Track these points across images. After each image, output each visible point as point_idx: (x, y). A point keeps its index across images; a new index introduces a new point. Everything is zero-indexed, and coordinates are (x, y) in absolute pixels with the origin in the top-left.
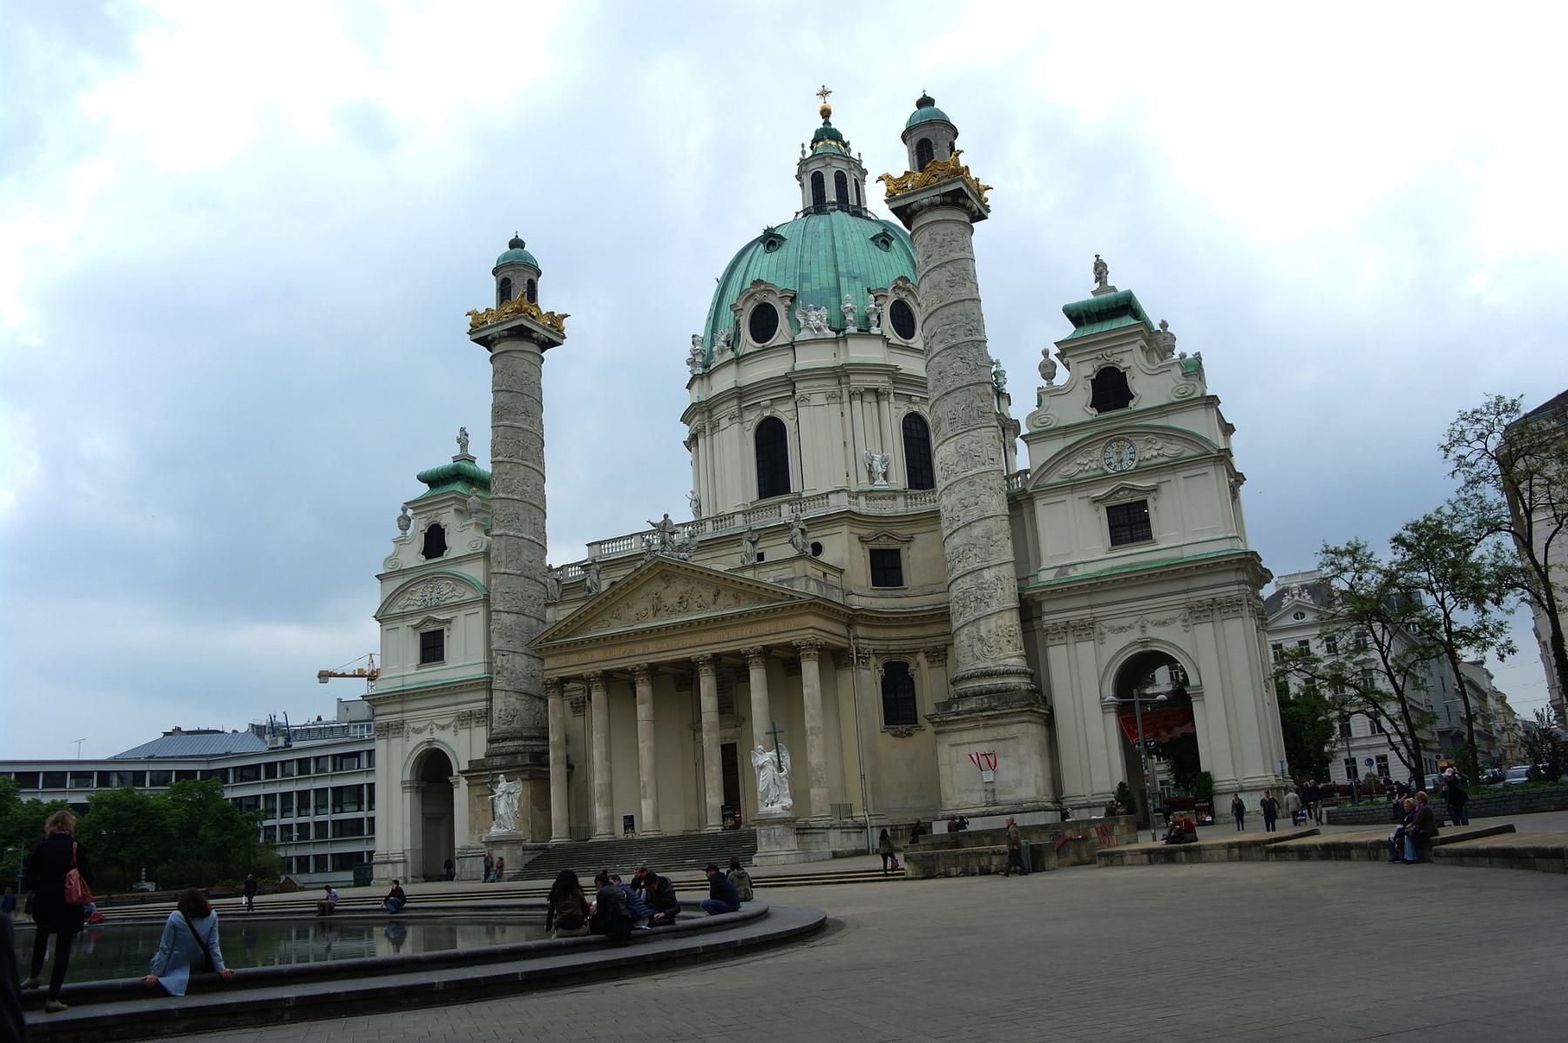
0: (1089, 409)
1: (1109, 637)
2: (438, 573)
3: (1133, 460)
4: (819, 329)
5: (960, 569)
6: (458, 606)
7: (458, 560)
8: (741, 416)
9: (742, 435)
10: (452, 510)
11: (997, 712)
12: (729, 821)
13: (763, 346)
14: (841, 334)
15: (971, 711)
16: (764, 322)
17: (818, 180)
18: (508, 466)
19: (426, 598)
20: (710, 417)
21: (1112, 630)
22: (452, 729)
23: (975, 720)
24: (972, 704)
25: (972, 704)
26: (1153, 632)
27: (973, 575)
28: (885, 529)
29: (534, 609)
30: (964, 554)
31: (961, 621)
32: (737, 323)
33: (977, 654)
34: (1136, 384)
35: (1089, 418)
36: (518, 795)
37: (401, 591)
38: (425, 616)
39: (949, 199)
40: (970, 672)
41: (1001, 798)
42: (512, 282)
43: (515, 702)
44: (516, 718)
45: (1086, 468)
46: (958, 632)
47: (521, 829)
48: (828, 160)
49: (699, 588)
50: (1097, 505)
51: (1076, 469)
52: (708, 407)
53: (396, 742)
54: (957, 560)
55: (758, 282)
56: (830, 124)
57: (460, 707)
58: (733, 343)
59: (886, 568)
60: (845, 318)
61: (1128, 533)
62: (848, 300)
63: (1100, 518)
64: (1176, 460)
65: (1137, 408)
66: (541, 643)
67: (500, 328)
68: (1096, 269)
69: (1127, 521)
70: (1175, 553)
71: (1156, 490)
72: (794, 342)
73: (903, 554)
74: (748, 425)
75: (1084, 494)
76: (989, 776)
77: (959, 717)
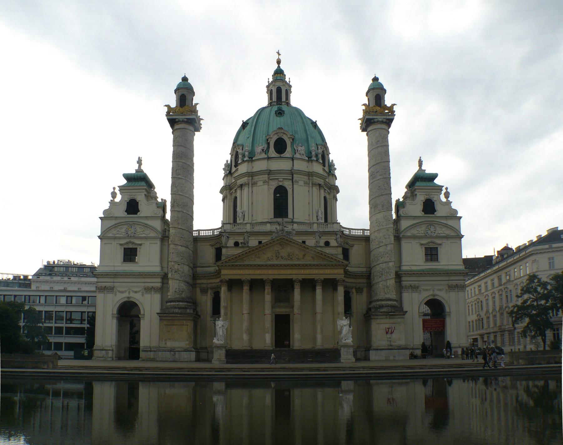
0: (421, 212)
2: (136, 222)
3: (435, 233)
4: (303, 155)
5: (381, 260)
6: (146, 238)
7: (146, 218)
8: (268, 182)
9: (269, 189)
11: (395, 313)
13: (280, 156)
14: (310, 159)
15: (384, 312)
16: (280, 146)
19: (128, 232)
20: (252, 179)
23: (386, 315)
24: (385, 310)
27: (386, 264)
28: (347, 240)
29: (191, 246)
30: (384, 256)
31: (380, 279)
33: (386, 292)
35: (422, 215)
37: (115, 226)
38: (129, 240)
40: (384, 298)
43: (183, 286)
44: (183, 294)
45: (420, 233)
46: (378, 283)
48: (284, 83)
50: (422, 246)
51: (416, 232)
52: (252, 175)
56: (280, 67)
58: (265, 151)
60: (311, 153)
61: (430, 257)
62: (312, 147)
63: (423, 251)
64: (448, 236)
65: (437, 215)
69: (430, 254)
70: (446, 268)
71: (441, 245)
72: (294, 157)
75: (417, 241)
77: (381, 314)
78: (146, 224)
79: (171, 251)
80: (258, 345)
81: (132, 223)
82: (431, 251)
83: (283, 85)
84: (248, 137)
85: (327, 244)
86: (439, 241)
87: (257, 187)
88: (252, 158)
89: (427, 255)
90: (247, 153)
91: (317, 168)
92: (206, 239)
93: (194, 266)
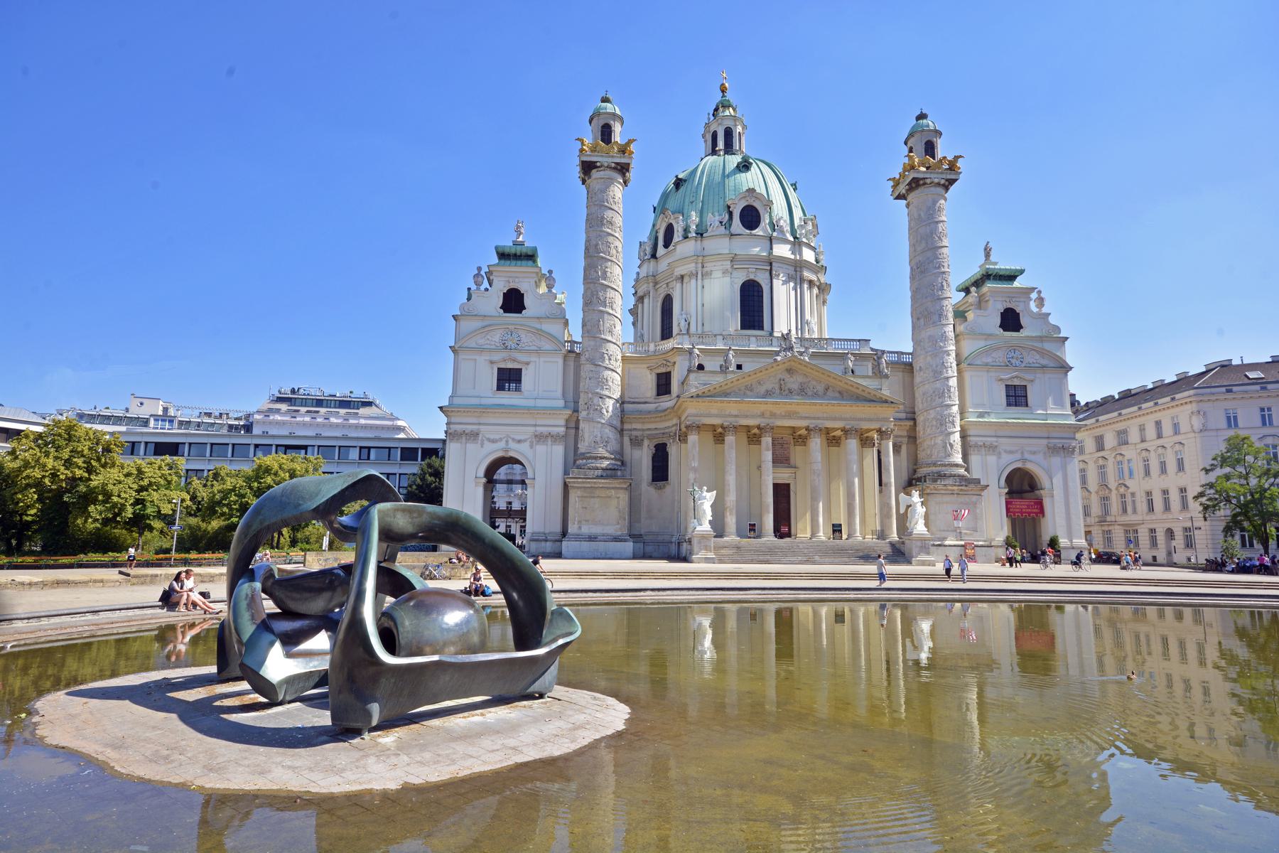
1: (1004, 456)
10: (533, 282)
11: (968, 488)
12: (837, 534)
16: (751, 218)
17: (729, 133)
18: (610, 263)
21: (1006, 451)
22: (527, 444)
25: (949, 481)
26: (1027, 456)
32: (731, 214)
34: (1024, 320)
36: (711, 503)
39: (947, 183)
42: (613, 129)
47: (618, 523)
49: (814, 383)
53: (471, 447)
54: (937, 397)
56: (725, 96)
57: (538, 428)
66: (692, 397)
67: (610, 160)
68: (985, 249)
71: (1032, 381)
74: (736, 280)
78: (537, 330)
81: (513, 327)
82: (1015, 390)
83: (736, 125)
84: (692, 202)
87: (712, 280)
88: (702, 235)
89: (1009, 396)
93: (623, 403)
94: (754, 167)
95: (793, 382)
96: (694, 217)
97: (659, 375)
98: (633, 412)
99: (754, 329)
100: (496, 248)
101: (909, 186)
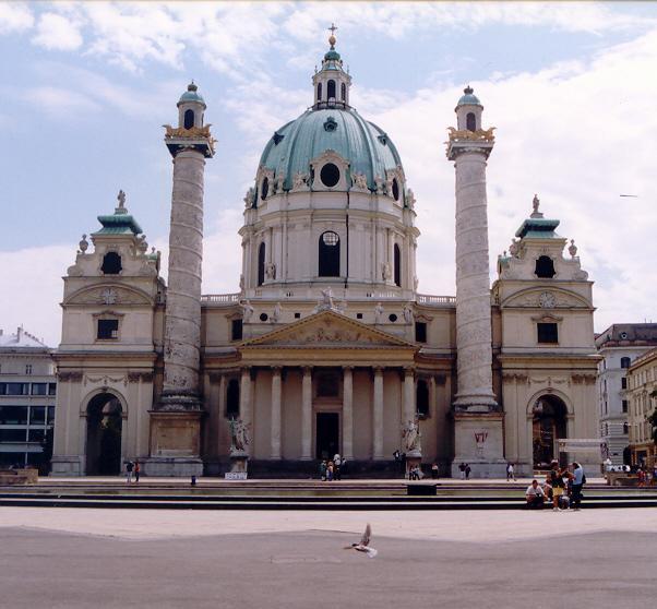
16: (330, 175)
17: (331, 85)
18: (189, 230)
22: (123, 382)
26: (553, 386)
32: (313, 172)
34: (557, 267)
37: (87, 290)
41: (484, 456)
55: (333, 151)
57: (131, 370)
59: (421, 332)
65: (559, 278)
67: (190, 143)
73: (428, 326)
76: (479, 445)
79: (169, 326)
80: (291, 457)
85: (393, 318)
86: (557, 315)
90: (280, 184)
91: (387, 206)
92: (219, 308)
93: (203, 346)
94: (341, 126)
95: (330, 332)
96: (281, 177)
97: (234, 322)
98: (210, 354)
99: (332, 276)
100: (99, 218)
101: (454, 153)
